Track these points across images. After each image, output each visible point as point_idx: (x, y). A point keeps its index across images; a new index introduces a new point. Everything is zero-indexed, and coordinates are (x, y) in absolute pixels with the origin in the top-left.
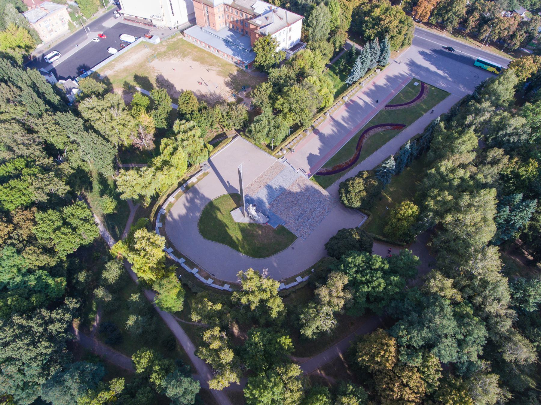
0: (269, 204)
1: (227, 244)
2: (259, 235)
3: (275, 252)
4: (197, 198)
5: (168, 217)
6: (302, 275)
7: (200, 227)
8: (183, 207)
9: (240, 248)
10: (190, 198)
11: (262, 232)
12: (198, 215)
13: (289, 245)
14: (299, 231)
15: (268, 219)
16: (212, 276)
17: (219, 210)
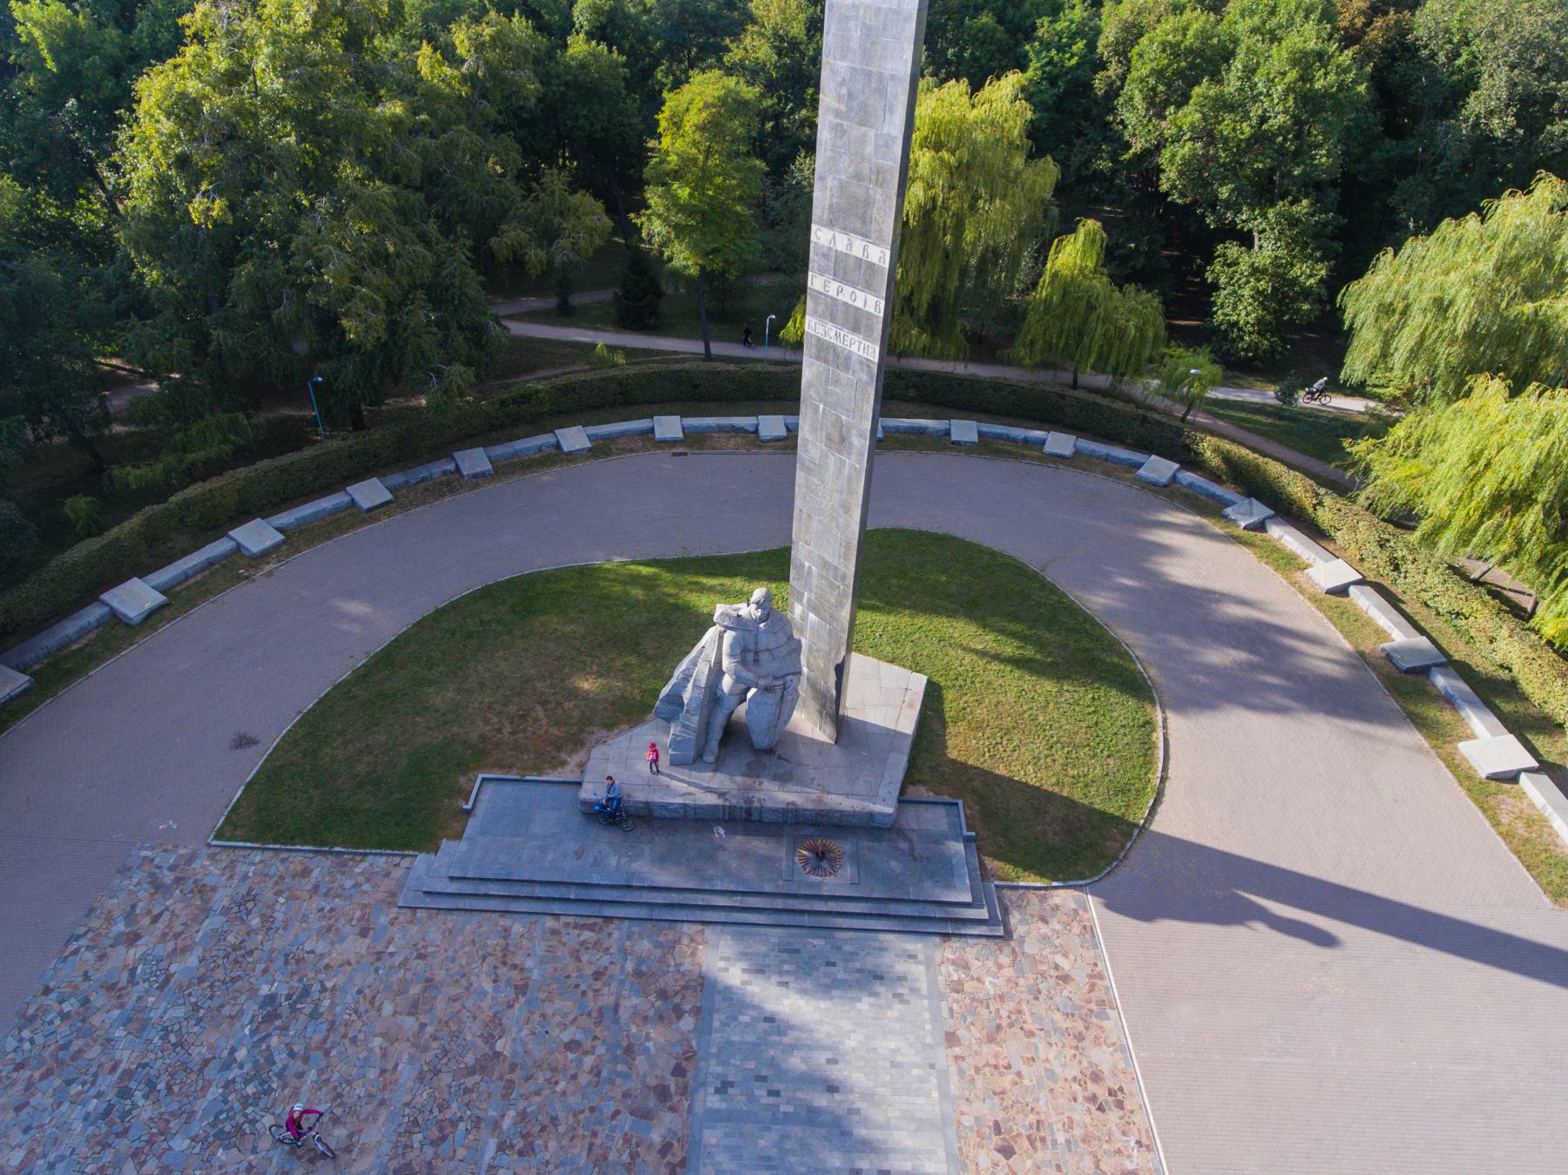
0: (702, 983)
1: (749, 556)
2: (583, 670)
3: (387, 658)
4: (1253, 667)
5: (1198, 519)
6: (118, 631)
7: (993, 554)
8: (1218, 585)
9: (645, 570)
10: (1292, 651)
11: (575, 694)
12: (1097, 602)
13: (290, 742)
14: (221, 899)
15: (593, 791)
16: (681, 450)
17: (1018, 663)
